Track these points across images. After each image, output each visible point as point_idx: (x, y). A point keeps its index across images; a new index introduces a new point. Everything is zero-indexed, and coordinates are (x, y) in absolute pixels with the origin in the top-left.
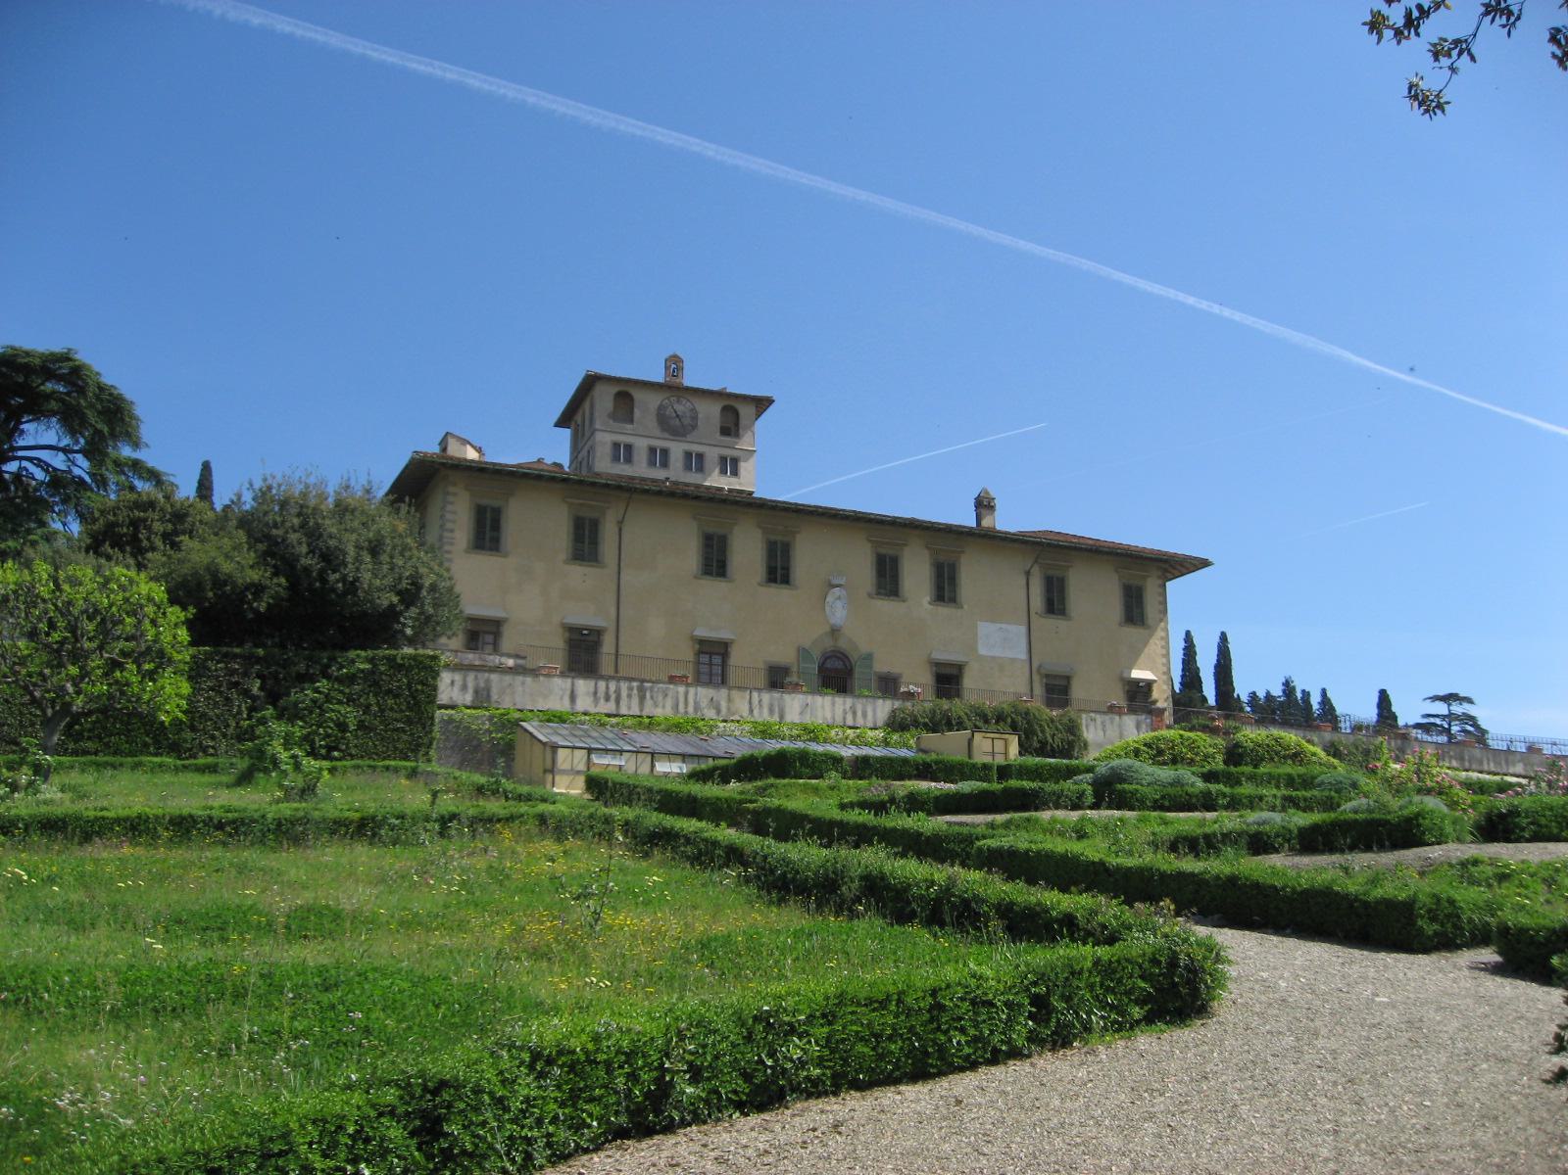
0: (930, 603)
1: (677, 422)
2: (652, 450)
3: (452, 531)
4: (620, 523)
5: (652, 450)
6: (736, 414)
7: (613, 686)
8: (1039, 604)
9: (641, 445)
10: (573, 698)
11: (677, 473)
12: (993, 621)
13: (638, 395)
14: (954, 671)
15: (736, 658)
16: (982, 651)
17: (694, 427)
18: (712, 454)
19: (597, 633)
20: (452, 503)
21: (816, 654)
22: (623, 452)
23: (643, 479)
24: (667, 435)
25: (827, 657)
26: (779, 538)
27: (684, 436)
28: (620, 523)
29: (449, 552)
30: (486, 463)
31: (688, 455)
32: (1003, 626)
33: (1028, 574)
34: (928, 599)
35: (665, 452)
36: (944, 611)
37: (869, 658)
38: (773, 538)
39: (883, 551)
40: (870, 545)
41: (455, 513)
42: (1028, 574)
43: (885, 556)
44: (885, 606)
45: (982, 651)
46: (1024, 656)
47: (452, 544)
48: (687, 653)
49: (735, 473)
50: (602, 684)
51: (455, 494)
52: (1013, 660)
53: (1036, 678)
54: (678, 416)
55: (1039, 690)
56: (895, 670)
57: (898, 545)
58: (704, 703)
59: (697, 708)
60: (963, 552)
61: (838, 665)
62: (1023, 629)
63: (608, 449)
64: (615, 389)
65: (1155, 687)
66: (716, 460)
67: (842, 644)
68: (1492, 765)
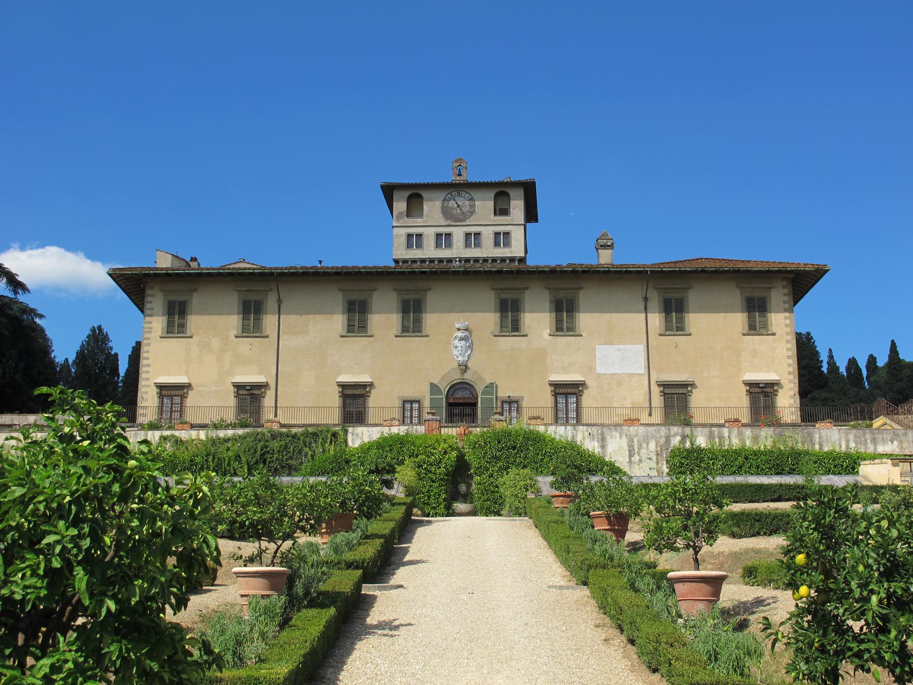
0: (550, 335)
1: (459, 211)
2: (439, 236)
3: (150, 323)
4: (280, 301)
5: (439, 236)
8: (658, 324)
9: (429, 234)
11: (458, 250)
12: (610, 343)
13: (425, 194)
15: (374, 401)
16: (600, 369)
17: (472, 213)
18: (488, 234)
19: (264, 386)
20: (151, 302)
21: (444, 388)
22: (415, 240)
23: (432, 261)
24: (450, 222)
25: (454, 388)
26: (412, 296)
27: (464, 220)
28: (280, 301)
29: (149, 339)
30: (157, 269)
31: (468, 235)
32: (621, 347)
34: (548, 331)
35: (449, 235)
36: (562, 341)
37: (491, 388)
38: (406, 297)
39: (504, 296)
40: (492, 294)
41: (152, 309)
42: (646, 299)
43: (506, 300)
44: (508, 342)
45: (600, 369)
46: (642, 370)
47: (150, 332)
48: (335, 400)
51: (153, 295)
52: (631, 375)
53: (656, 390)
54: (458, 206)
55: (658, 401)
56: (514, 394)
57: (518, 289)
60: (581, 288)
61: (466, 394)
62: (641, 348)
63: (404, 240)
64: (407, 194)
66: (492, 236)
67: (468, 376)
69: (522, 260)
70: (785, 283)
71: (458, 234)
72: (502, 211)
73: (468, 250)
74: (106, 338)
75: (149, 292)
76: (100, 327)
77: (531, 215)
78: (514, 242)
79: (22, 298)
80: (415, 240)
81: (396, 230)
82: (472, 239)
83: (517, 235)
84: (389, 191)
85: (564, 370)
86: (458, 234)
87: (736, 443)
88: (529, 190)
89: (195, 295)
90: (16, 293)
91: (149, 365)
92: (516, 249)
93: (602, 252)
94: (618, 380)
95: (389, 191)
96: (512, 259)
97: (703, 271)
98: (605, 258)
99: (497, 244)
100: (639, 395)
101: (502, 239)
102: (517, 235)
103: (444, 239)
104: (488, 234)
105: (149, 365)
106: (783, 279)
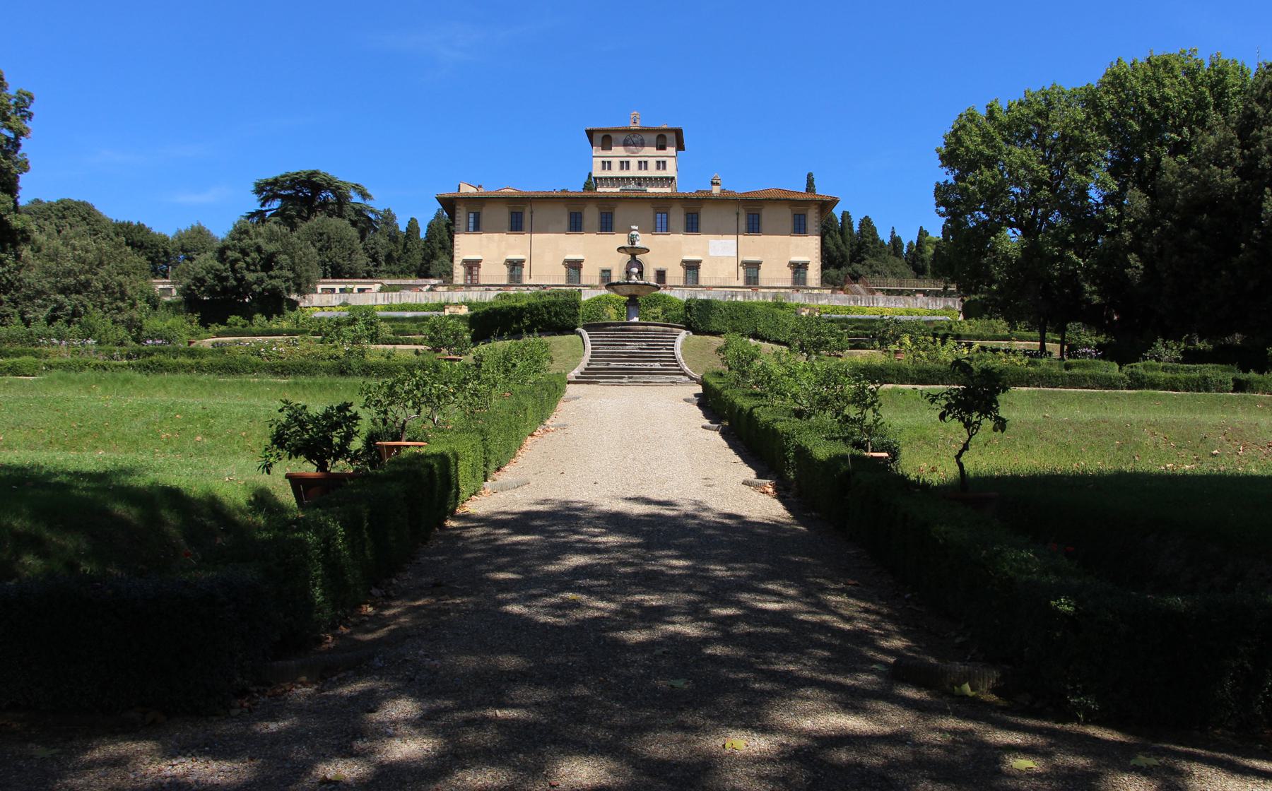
4: (532, 212)
6: (665, 137)
7: (390, 294)
10: (376, 300)
13: (613, 136)
14: (695, 265)
16: (712, 254)
18: (652, 163)
19: (523, 261)
28: (532, 212)
31: (640, 162)
33: (738, 214)
42: (738, 214)
49: (664, 168)
50: (386, 294)
55: (741, 270)
58: (423, 299)
59: (420, 300)
62: (735, 241)
63: (600, 165)
64: (601, 135)
65: (809, 266)
66: (655, 163)
68: (807, 301)
69: (673, 179)
70: (816, 206)
71: (634, 162)
72: (662, 147)
73: (640, 171)
74: (394, 217)
75: (458, 207)
76: (389, 210)
77: (680, 147)
78: (667, 167)
79: (368, 202)
80: (607, 165)
81: (594, 159)
82: (643, 165)
83: (671, 164)
84: (590, 134)
85: (691, 253)
86: (634, 162)
87: (755, 299)
88: (678, 133)
89: (484, 208)
90: (365, 199)
91: (458, 249)
92: (671, 171)
93: (714, 187)
94: (720, 259)
95: (590, 134)
96: (667, 178)
97: (770, 199)
98: (716, 190)
99: (658, 168)
100: (732, 267)
101: (661, 165)
102: (671, 164)
103: (625, 165)
104: (652, 163)
105: (458, 249)
106: (816, 204)
